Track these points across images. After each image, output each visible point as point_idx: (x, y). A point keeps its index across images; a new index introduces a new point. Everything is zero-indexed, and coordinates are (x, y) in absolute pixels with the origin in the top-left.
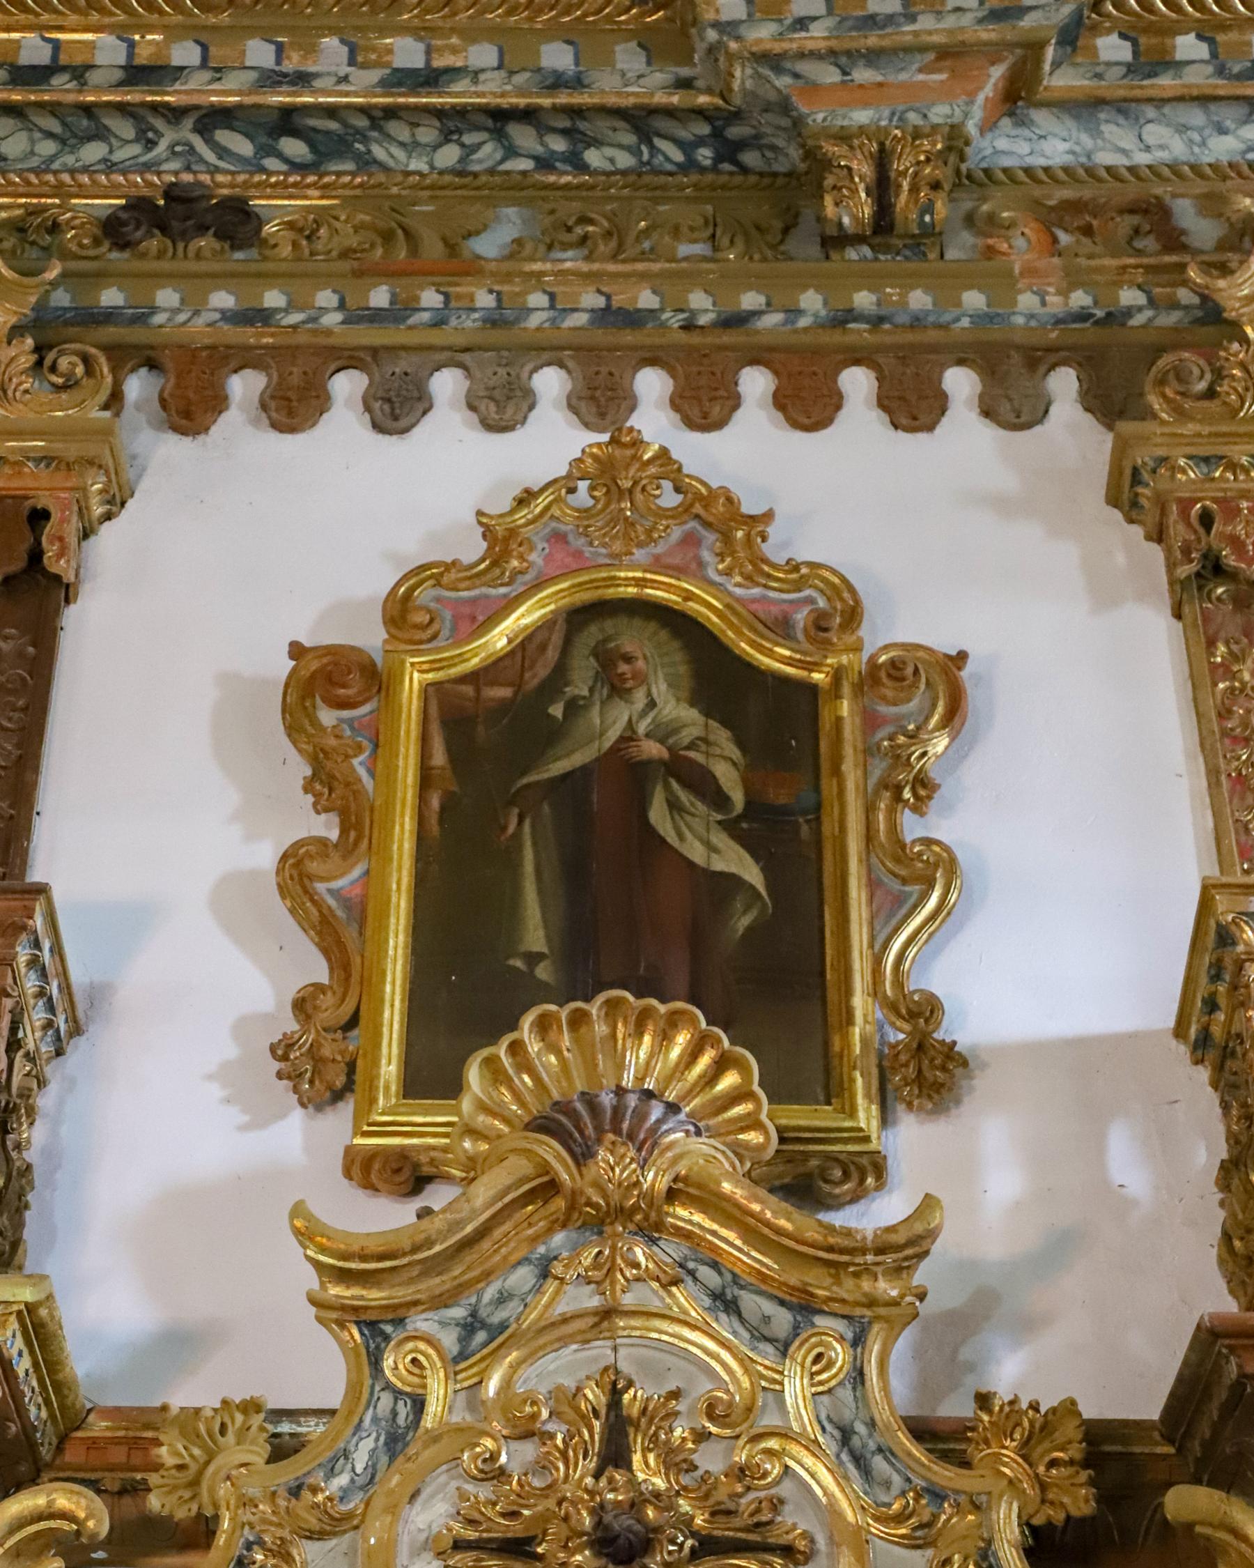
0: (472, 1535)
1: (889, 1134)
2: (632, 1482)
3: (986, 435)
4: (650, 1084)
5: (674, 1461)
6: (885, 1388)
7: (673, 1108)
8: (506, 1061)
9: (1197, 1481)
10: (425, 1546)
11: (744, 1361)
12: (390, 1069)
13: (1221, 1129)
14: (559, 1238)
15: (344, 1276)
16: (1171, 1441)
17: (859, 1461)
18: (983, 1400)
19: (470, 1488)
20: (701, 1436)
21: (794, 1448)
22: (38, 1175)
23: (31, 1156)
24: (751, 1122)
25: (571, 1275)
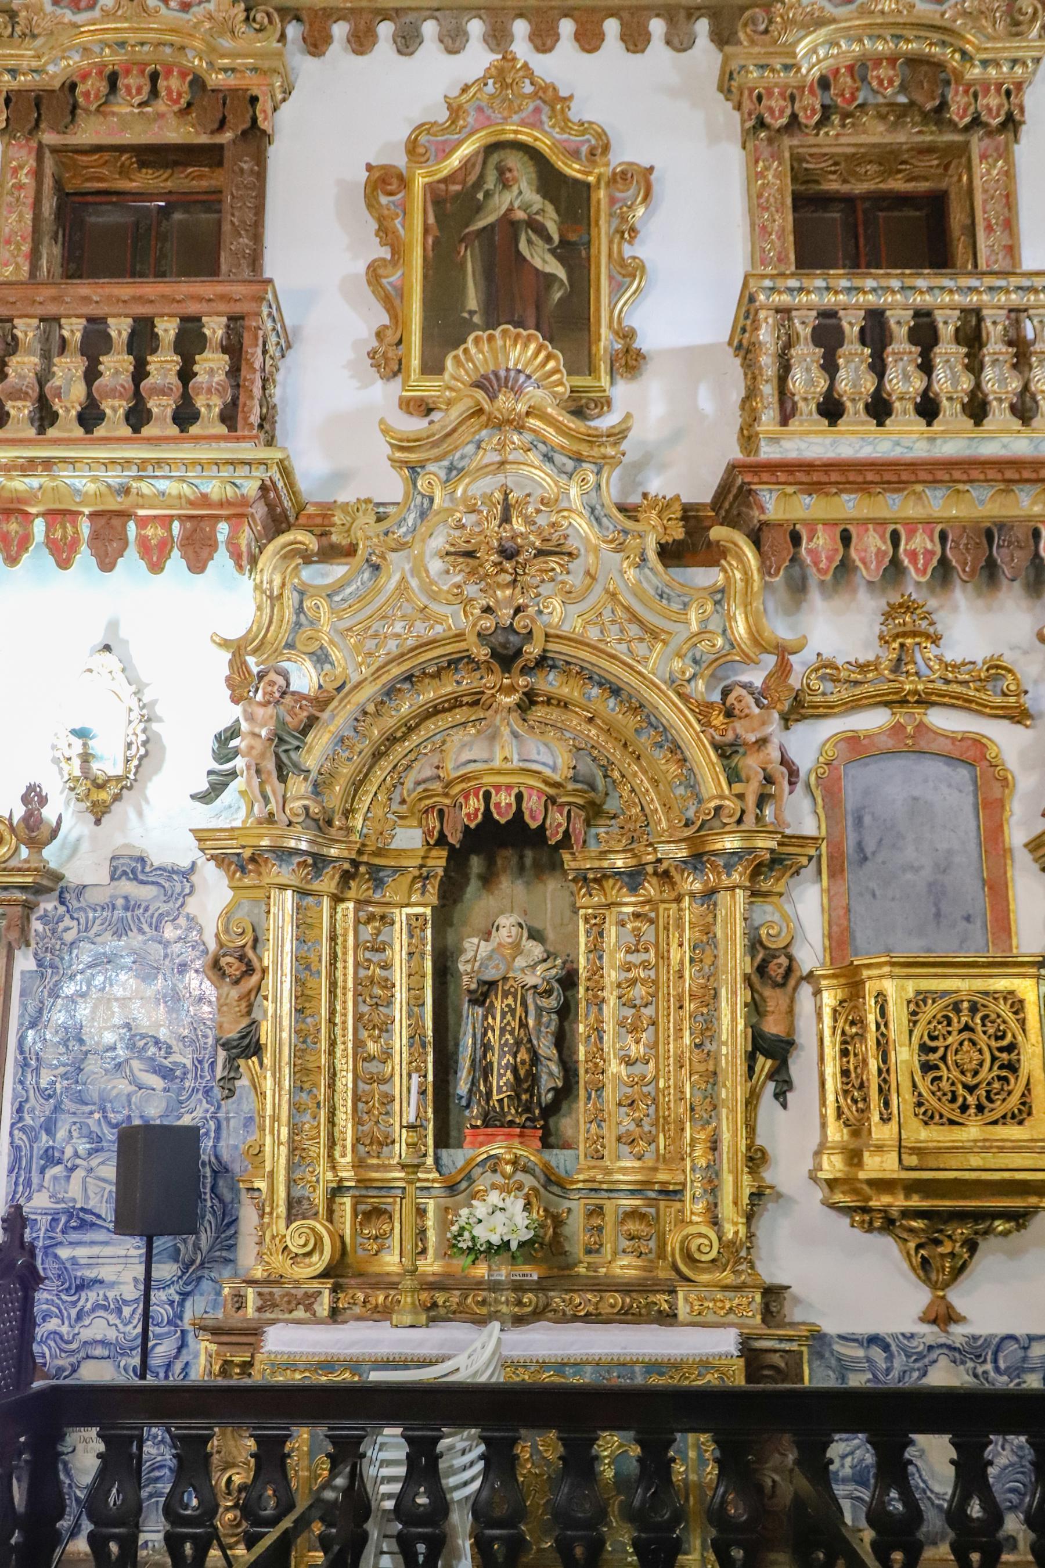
0: (453, 550)
1: (613, 389)
2: (512, 529)
3: (667, 53)
4: (519, 367)
5: (529, 521)
6: (608, 491)
7: (529, 377)
8: (462, 357)
9: (722, 524)
10: (436, 554)
11: (556, 483)
12: (415, 362)
13: (743, 385)
14: (484, 432)
15: (402, 449)
16: (713, 510)
17: (597, 519)
18: (645, 495)
19: (452, 532)
20: (538, 511)
21: (573, 515)
22: (279, 407)
23: (276, 400)
24: (561, 383)
25: (489, 448)
